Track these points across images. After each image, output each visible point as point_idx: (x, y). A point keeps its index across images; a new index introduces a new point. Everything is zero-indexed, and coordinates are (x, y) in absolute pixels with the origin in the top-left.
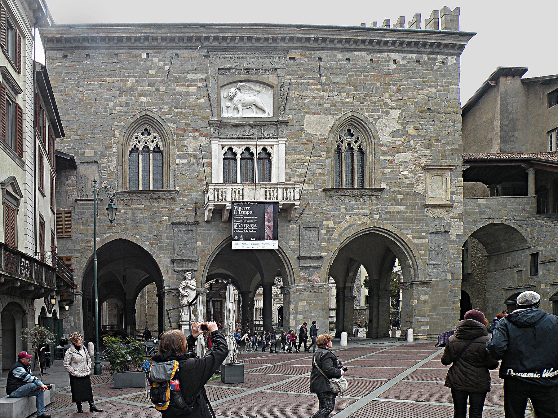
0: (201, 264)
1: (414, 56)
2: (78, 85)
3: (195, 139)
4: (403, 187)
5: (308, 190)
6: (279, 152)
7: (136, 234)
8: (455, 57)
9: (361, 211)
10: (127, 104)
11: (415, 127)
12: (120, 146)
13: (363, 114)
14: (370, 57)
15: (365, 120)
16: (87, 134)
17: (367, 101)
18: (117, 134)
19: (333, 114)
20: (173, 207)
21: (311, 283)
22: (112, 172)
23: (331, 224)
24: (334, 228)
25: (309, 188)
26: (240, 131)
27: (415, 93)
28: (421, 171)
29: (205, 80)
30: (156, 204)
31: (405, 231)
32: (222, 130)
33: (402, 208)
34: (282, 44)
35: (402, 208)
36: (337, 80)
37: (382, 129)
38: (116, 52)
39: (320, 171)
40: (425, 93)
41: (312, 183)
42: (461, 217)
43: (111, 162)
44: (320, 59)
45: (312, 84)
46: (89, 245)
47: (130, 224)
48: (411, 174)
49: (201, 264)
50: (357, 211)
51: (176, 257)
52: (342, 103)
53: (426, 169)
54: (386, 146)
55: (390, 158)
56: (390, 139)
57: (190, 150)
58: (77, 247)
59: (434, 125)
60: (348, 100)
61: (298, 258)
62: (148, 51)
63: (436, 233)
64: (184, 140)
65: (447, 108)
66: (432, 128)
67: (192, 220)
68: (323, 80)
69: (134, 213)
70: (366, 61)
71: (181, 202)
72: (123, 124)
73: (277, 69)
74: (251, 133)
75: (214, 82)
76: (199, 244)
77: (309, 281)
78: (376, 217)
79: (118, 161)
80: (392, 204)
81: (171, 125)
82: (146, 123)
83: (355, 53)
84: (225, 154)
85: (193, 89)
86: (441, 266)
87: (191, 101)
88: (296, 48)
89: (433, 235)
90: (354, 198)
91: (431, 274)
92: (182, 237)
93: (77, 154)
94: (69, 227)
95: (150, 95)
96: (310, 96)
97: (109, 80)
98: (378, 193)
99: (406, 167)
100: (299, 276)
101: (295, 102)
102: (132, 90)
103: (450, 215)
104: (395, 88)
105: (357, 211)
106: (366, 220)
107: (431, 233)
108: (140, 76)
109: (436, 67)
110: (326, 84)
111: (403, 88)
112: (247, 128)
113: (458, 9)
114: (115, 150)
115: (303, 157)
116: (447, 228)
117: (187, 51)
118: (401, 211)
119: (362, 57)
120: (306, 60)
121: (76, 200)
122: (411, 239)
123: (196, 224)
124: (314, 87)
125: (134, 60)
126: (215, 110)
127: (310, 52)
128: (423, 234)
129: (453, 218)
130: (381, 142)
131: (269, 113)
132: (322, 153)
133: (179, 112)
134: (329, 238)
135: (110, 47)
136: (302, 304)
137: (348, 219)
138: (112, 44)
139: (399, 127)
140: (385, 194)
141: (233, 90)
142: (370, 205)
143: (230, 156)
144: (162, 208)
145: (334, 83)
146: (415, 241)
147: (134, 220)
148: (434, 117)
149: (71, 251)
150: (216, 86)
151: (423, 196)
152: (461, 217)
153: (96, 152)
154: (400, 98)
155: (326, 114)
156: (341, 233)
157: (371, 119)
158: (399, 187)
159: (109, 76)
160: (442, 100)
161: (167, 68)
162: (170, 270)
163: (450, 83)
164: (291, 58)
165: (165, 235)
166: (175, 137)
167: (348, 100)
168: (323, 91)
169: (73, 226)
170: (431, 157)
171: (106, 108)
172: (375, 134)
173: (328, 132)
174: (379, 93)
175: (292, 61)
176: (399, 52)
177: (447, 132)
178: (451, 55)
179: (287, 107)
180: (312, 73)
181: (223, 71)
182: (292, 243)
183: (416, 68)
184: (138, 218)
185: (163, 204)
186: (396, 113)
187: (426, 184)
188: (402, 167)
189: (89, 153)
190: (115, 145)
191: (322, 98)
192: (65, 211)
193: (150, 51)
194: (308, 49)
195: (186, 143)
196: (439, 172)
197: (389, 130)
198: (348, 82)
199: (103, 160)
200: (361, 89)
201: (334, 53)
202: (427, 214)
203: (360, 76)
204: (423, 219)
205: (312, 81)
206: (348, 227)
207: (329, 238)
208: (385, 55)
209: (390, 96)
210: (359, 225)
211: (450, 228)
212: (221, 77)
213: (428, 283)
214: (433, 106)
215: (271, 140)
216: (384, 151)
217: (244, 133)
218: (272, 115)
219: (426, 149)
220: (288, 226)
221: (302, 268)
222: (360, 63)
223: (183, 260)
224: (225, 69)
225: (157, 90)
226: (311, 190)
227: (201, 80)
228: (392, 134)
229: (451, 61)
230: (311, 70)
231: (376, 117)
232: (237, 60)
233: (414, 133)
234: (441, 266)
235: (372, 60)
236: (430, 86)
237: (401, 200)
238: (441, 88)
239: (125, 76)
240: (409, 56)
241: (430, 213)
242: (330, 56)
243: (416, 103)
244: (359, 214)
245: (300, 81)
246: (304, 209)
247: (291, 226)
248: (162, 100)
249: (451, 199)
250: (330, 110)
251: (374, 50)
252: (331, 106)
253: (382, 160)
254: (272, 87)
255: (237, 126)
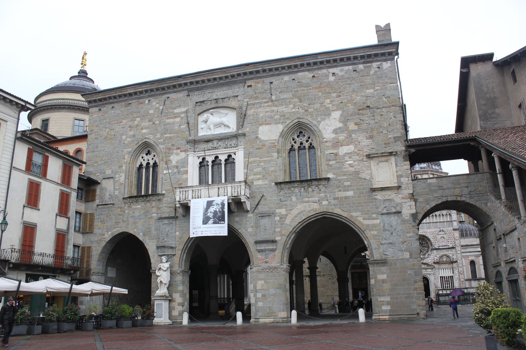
0: (178, 250)
1: (351, 67)
2: (106, 128)
3: (177, 154)
4: (349, 175)
5: (263, 185)
6: (239, 158)
7: (134, 228)
8: (389, 62)
9: (311, 199)
10: (134, 136)
11: (356, 123)
12: (128, 164)
13: (307, 119)
14: (312, 75)
15: (309, 123)
16: (109, 159)
17: (311, 108)
18: (126, 157)
19: (282, 123)
20: (160, 206)
21: (268, 265)
22: (122, 184)
23: (283, 211)
24: (287, 215)
25: (263, 183)
26: (210, 145)
27: (353, 96)
28: (365, 159)
29: (186, 112)
30: (148, 205)
31: (354, 214)
32: (196, 146)
33: (350, 193)
34: (240, 78)
35: (350, 193)
36: (285, 96)
37: (325, 129)
38: (130, 102)
39: (273, 169)
40: (363, 94)
41: (266, 179)
42: (412, 197)
43: (121, 176)
44: (271, 83)
45: (265, 102)
46: (103, 237)
47: (131, 220)
48: (356, 163)
49: (178, 250)
50: (306, 199)
51: (161, 245)
52: (290, 113)
53: (369, 157)
54: (330, 142)
55: (335, 151)
56: (333, 136)
57: (174, 163)
58: (96, 239)
59: (374, 119)
60: (294, 110)
61: (257, 242)
62: (149, 99)
63: (387, 214)
64: (170, 156)
65: (386, 103)
66: (372, 122)
67: (173, 215)
68: (274, 98)
69: (134, 213)
70: (308, 78)
71: (165, 202)
72: (130, 149)
73: (237, 96)
74: (218, 145)
75: (192, 112)
76: (177, 233)
77: (266, 262)
78: (325, 203)
79: (125, 176)
80: (340, 191)
81: (161, 146)
82: (146, 147)
83: (300, 74)
84: (200, 163)
85: (178, 120)
86: (397, 245)
87: (176, 128)
88: (251, 79)
89: (384, 216)
90: (303, 189)
91: (386, 253)
92: (165, 229)
93: (101, 173)
94: (91, 225)
95: (149, 128)
96: (262, 112)
97: (124, 121)
98: (324, 183)
99: (350, 157)
100: (257, 258)
101: (251, 118)
102: (138, 125)
103: (400, 196)
104: (335, 95)
105: (306, 199)
106: (316, 206)
107: (382, 214)
108: (143, 116)
109: (372, 72)
110: (276, 101)
111: (343, 94)
112: (215, 142)
113: (388, 25)
114: (124, 168)
115: (258, 159)
116: (398, 209)
117: (175, 94)
118: (349, 197)
119: (305, 76)
120: (260, 85)
121: (98, 205)
122: (362, 221)
123: (175, 218)
124: (266, 104)
125: (141, 106)
126: (192, 132)
127: (263, 79)
128: (374, 216)
129: (403, 198)
130: (325, 140)
131: (233, 128)
132: (273, 154)
133: (167, 137)
134: (282, 224)
135: (125, 100)
136: (260, 284)
137: (299, 207)
138: (126, 98)
139: (340, 125)
140: (331, 183)
141: (205, 116)
142: (319, 193)
143: (202, 164)
144: (153, 207)
145: (282, 99)
146: (366, 222)
147: (133, 217)
148: (374, 112)
149: (92, 242)
150: (194, 115)
151: (370, 181)
152: (412, 197)
153: (112, 171)
154: (340, 102)
155: (276, 123)
156: (293, 219)
157: (315, 122)
158: (345, 175)
159: (124, 119)
160: (380, 98)
161: (161, 108)
162: (156, 255)
163: (387, 83)
164: (248, 86)
165: (153, 228)
166: (164, 155)
167: (294, 110)
168: (274, 106)
169: (95, 224)
170: (375, 147)
171: (120, 140)
172: (319, 133)
173: (278, 137)
174: (321, 101)
175: (250, 88)
176: (336, 66)
177: (388, 123)
178: (385, 60)
179: (245, 123)
180: (265, 95)
181: (199, 104)
182: (250, 230)
183: (353, 76)
184: (136, 216)
185: (154, 204)
186: (336, 115)
187: (371, 170)
188: (347, 158)
189: (108, 172)
190: (125, 165)
191: (273, 111)
192: (90, 214)
193: (151, 98)
194: (261, 77)
195: (171, 158)
196: (384, 159)
197: (331, 129)
198: (295, 96)
199: (117, 176)
200: (305, 99)
201: (282, 77)
202: (376, 197)
203: (303, 90)
204: (372, 202)
205: (265, 100)
206: (299, 214)
207: (282, 224)
208: (324, 71)
209: (331, 101)
210: (309, 211)
211: (401, 208)
212: (197, 108)
213: (383, 262)
214: (371, 103)
215: (233, 149)
216: (328, 146)
217: (213, 146)
218: (235, 129)
219: (368, 140)
220: (247, 216)
221: (260, 251)
222: (303, 81)
223: (164, 247)
224: (201, 102)
225: (154, 123)
226: (265, 184)
227: (183, 113)
228: (335, 131)
229: (386, 65)
230: (264, 93)
231: (319, 119)
232: (208, 95)
233: (356, 128)
234: (397, 245)
235: (313, 76)
236: (367, 88)
237: (348, 186)
238: (379, 88)
239: (134, 118)
240: (346, 68)
241: (379, 196)
242: (279, 80)
243: (355, 103)
244: (309, 202)
245: (255, 102)
246: (259, 202)
247: (249, 215)
248: (157, 130)
249: (399, 181)
250: (280, 120)
251: (315, 69)
252: (281, 116)
253: (327, 154)
254: (235, 109)
255: (208, 141)
